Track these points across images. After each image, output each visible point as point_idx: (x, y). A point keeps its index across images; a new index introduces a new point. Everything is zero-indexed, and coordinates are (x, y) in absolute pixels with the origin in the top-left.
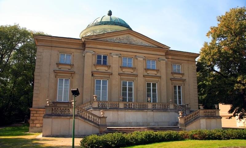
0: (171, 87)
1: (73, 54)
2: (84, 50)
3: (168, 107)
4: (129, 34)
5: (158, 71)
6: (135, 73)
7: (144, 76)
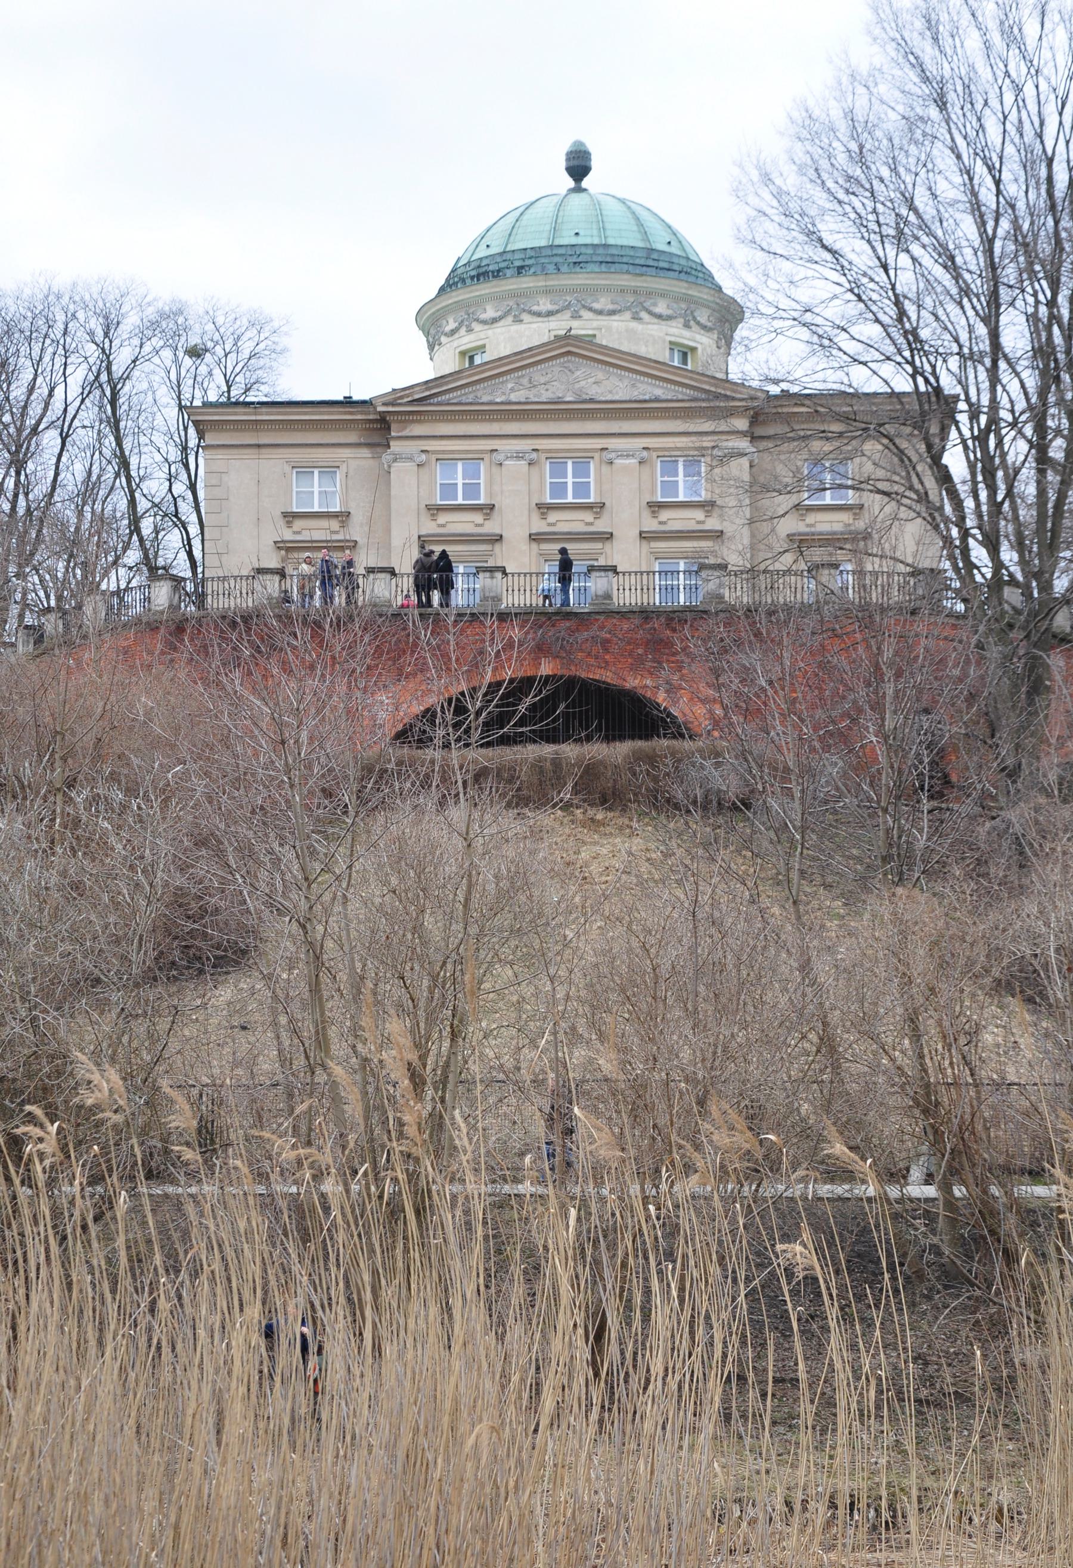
1: (344, 468)
4: (569, 353)
6: (601, 526)
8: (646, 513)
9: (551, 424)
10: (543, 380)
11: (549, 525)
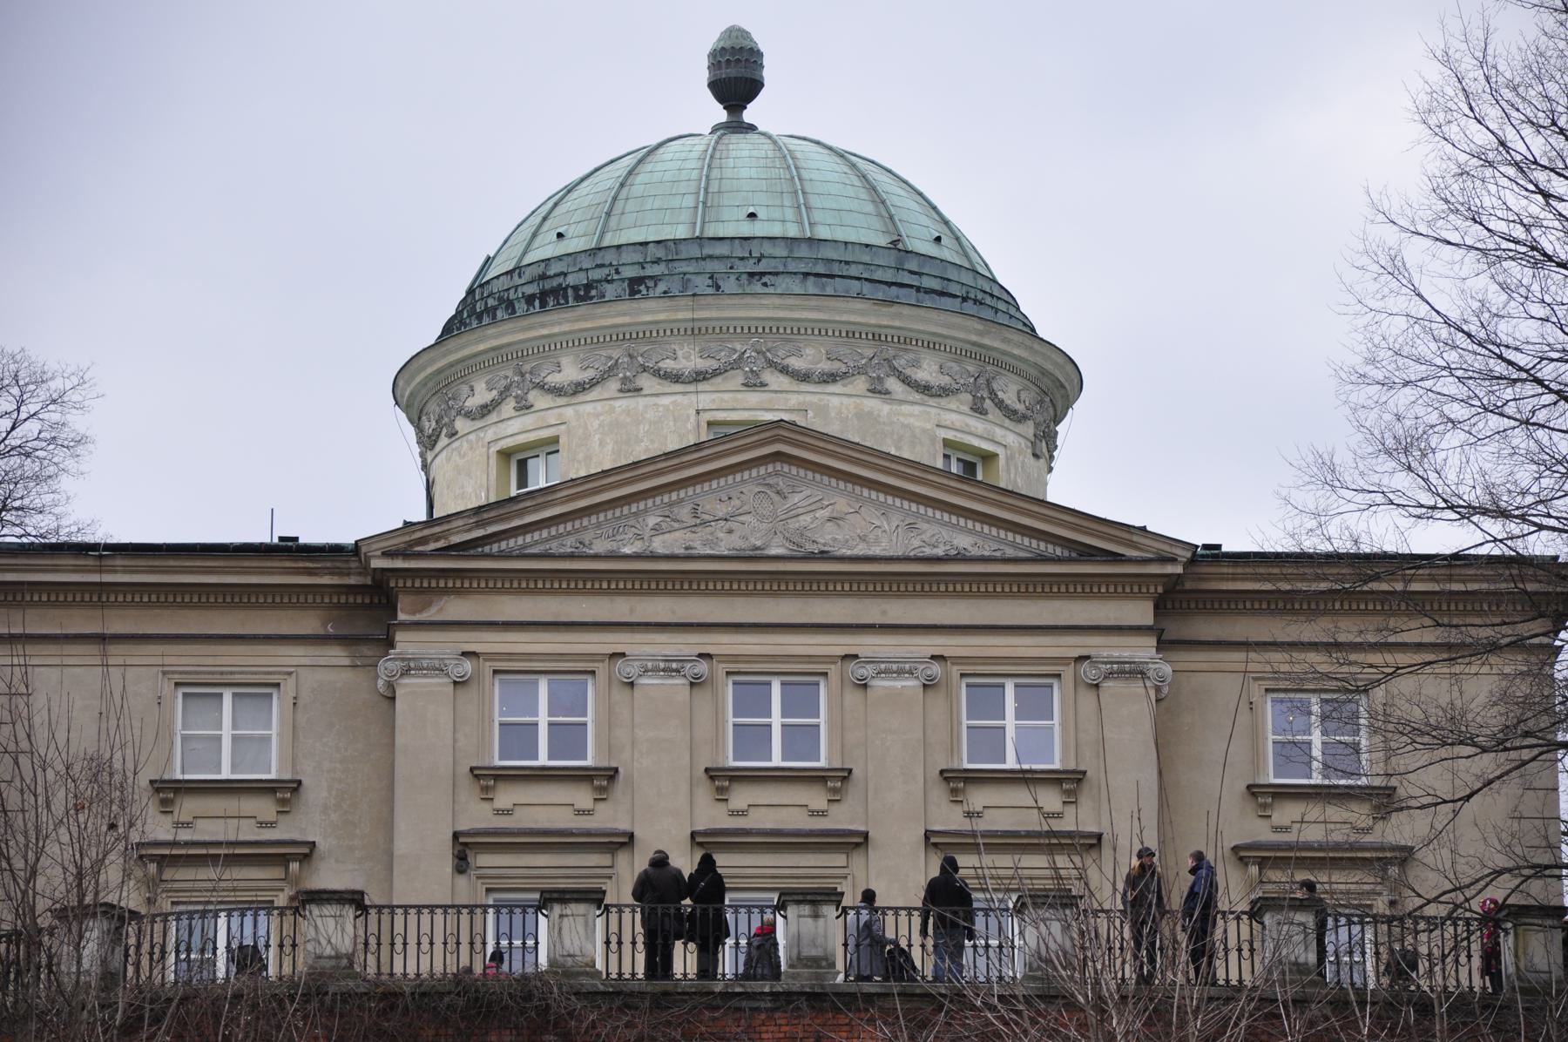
1: (289, 686)
4: (778, 456)
6: (842, 818)
7: (928, 835)
8: (939, 793)
9: (739, 602)
10: (722, 510)
11: (734, 813)
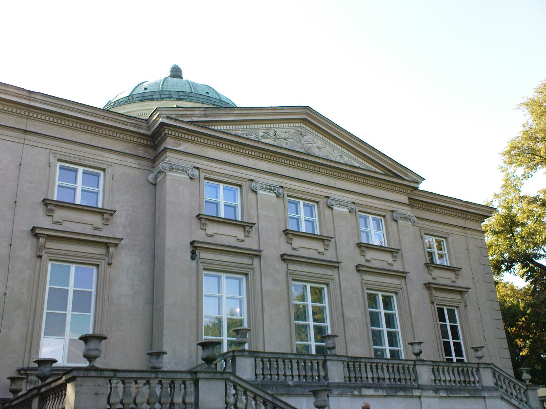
0: (430, 312)
1: (109, 171)
2: (154, 161)
3: (477, 379)
4: (304, 120)
5: (393, 252)
